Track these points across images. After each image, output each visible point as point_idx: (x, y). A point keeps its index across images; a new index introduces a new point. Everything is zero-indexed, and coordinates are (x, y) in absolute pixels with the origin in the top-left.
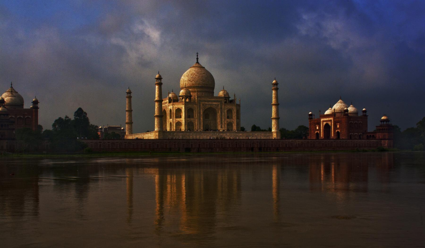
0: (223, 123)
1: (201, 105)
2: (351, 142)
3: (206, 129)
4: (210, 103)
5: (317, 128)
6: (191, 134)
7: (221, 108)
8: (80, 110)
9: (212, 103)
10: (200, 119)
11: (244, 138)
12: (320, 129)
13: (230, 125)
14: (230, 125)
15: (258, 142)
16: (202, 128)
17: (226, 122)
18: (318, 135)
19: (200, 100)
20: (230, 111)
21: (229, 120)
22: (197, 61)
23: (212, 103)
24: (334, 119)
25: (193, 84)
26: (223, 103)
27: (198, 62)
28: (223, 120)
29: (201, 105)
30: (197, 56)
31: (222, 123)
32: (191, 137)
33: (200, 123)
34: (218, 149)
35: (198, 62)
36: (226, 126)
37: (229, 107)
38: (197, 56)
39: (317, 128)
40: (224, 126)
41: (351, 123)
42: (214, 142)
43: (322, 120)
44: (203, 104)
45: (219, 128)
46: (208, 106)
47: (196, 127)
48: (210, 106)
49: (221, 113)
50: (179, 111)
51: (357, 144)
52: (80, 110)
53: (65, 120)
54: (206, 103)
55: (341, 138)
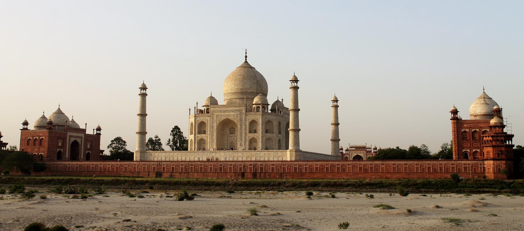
0: (243, 139)
1: (215, 117)
2: (417, 165)
4: (226, 114)
7: (241, 120)
11: (244, 159)
13: (252, 141)
14: (252, 141)
16: (215, 147)
20: (253, 123)
21: (252, 135)
22: (246, 59)
26: (244, 111)
27: (246, 62)
28: (243, 135)
31: (241, 139)
35: (246, 62)
36: (247, 143)
40: (245, 142)
41: (465, 131)
45: (238, 146)
46: (223, 118)
47: (208, 146)
48: (226, 117)
49: (241, 125)
51: (429, 168)
52: (176, 128)
53: (156, 140)
54: (222, 114)
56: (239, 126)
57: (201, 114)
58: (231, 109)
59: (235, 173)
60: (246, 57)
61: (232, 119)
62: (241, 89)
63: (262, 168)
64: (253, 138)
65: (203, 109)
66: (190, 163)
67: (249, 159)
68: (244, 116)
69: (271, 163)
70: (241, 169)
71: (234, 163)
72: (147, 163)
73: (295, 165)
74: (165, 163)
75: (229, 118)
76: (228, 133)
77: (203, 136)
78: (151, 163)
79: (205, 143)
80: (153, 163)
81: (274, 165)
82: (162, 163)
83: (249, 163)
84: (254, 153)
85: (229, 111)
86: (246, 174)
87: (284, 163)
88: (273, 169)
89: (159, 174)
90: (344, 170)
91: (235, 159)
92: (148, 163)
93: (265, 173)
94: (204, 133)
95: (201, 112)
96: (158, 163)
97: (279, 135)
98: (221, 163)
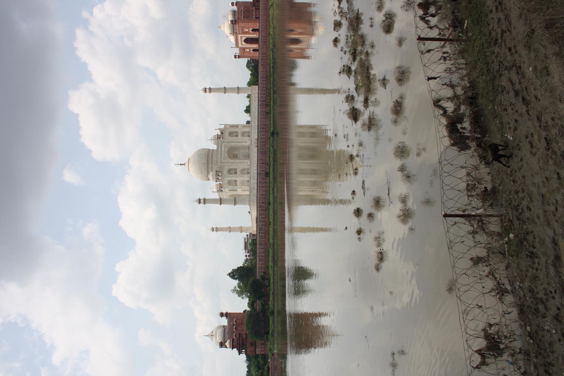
3: (248, 156)
5: (248, 50)
10: (238, 163)
12: (249, 48)
14: (243, 134)
16: (247, 161)
18: (255, 50)
19: (220, 162)
20: (231, 134)
21: (239, 135)
24: (239, 34)
27: (184, 164)
31: (242, 142)
32: (256, 171)
33: (242, 163)
34: (267, 146)
36: (245, 138)
37: (226, 135)
39: (248, 50)
43: (240, 46)
45: (247, 144)
46: (226, 155)
48: (226, 153)
49: (232, 142)
50: (230, 183)
55: (258, 28)
67: (257, 118)
88: (263, 94)
89: (267, 174)
90: (264, 54)
91: (257, 127)
94: (236, 173)
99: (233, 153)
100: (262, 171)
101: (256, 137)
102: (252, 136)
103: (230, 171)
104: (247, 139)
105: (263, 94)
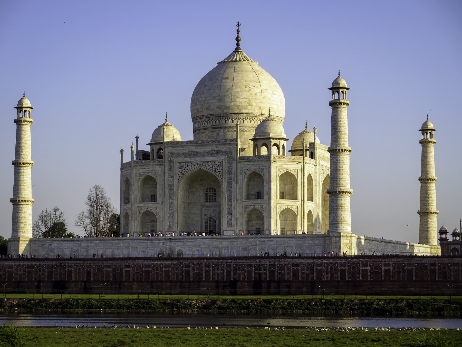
0: (234, 212)
1: (176, 166)
4: (198, 159)
6: (93, 245)
7: (230, 173)
8: (96, 187)
9: (203, 159)
10: (171, 204)
11: (233, 253)
15: (250, 266)
17: (240, 210)
19: (172, 154)
21: (251, 204)
22: (238, 45)
23: (203, 159)
25: (198, 110)
28: (234, 203)
29: (176, 166)
30: (238, 31)
31: (230, 213)
33: (171, 215)
34: (135, 286)
35: (237, 49)
36: (243, 220)
38: (238, 31)
42: (127, 266)
44: (179, 163)
45: (224, 226)
48: (197, 168)
54: (188, 159)
56: (225, 185)
57: (144, 161)
58: (208, 149)
59: (217, 282)
60: (238, 39)
61: (211, 171)
62: (228, 108)
63: (272, 272)
64: (255, 210)
65: (148, 149)
66: (123, 263)
67: (245, 254)
68: (234, 164)
69: (291, 261)
70: (228, 272)
71: (215, 262)
72: (34, 263)
73: (342, 265)
74: (71, 263)
75: (203, 168)
76: (202, 199)
77: (151, 206)
78: (42, 263)
79: (154, 221)
80: (46, 263)
81: (297, 265)
82: (67, 263)
83: (246, 261)
84: (257, 241)
85: (205, 154)
86: (239, 284)
87: (319, 261)
91: (216, 253)
92: (38, 263)
93: (278, 282)
94: (153, 198)
95: (144, 156)
96: (58, 263)
97: (307, 203)
98: (187, 262)
99: (206, 185)
100: (70, 273)
101: (188, 253)
102: (189, 243)
103: (149, 181)
104: (241, 224)
105: (296, 274)
